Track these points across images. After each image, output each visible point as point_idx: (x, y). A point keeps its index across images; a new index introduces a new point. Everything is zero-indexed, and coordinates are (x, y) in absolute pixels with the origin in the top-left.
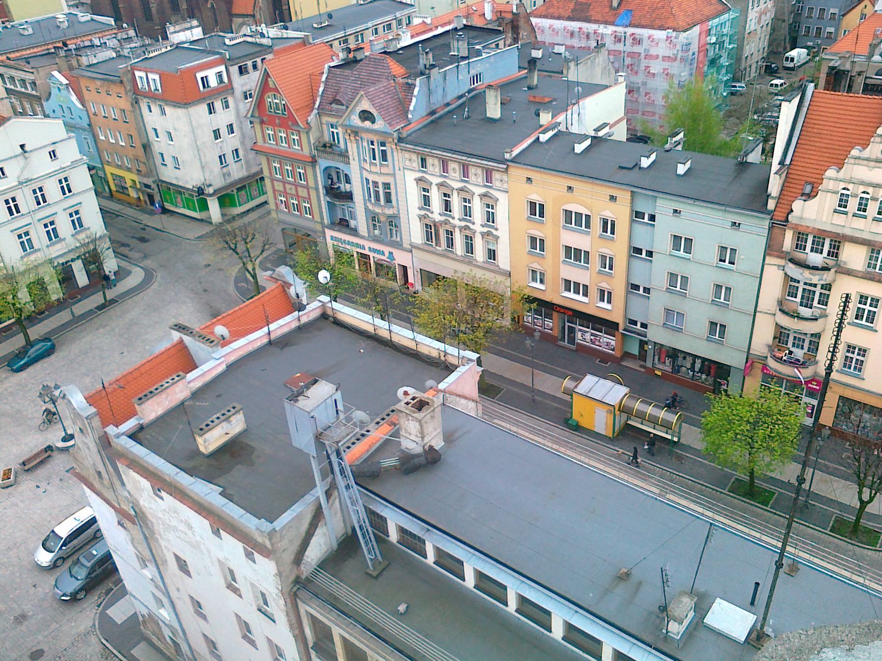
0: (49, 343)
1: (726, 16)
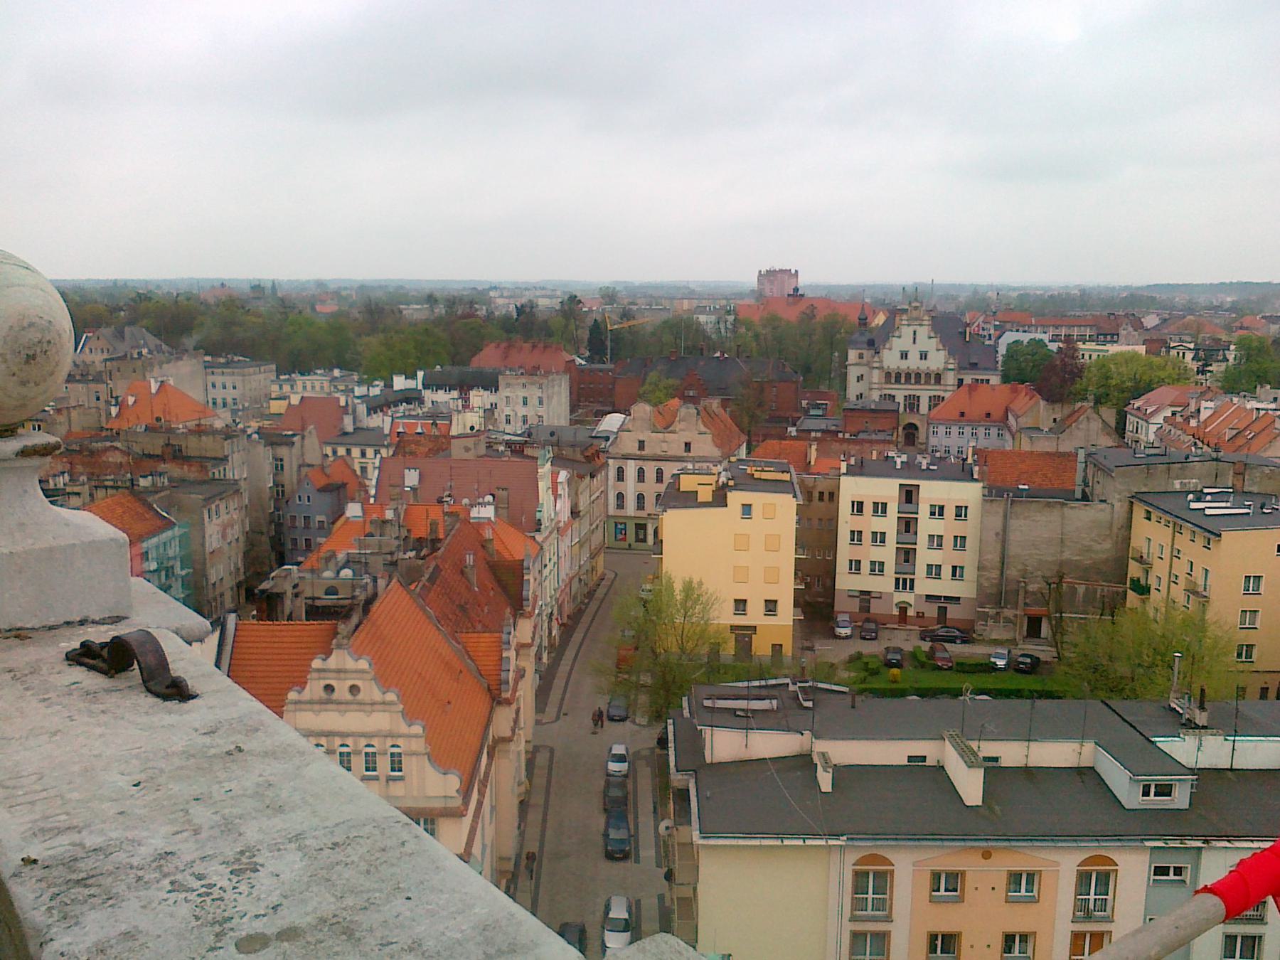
1: (169, 533)
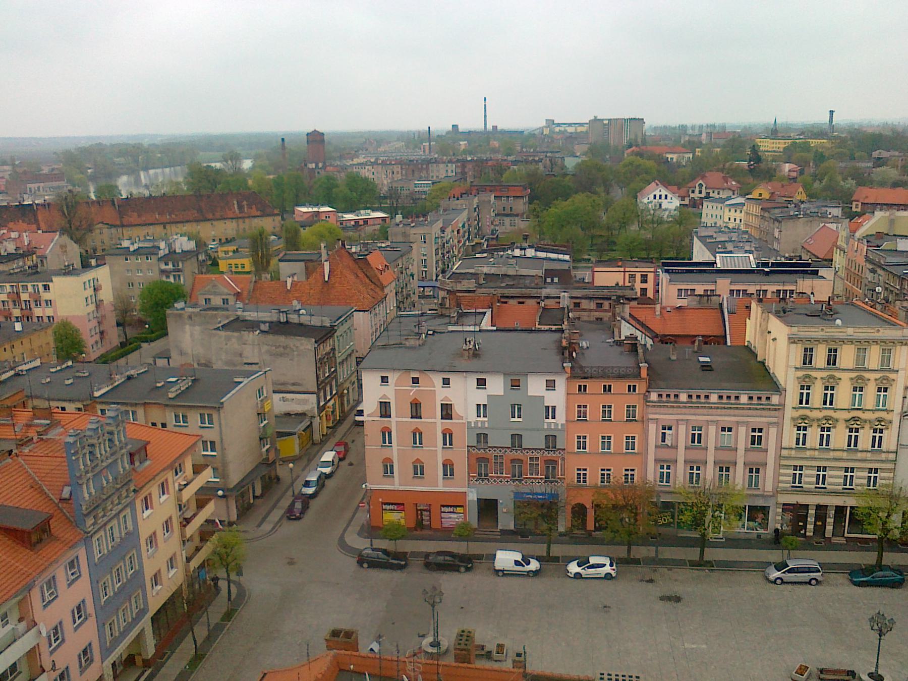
0: (899, 577)
